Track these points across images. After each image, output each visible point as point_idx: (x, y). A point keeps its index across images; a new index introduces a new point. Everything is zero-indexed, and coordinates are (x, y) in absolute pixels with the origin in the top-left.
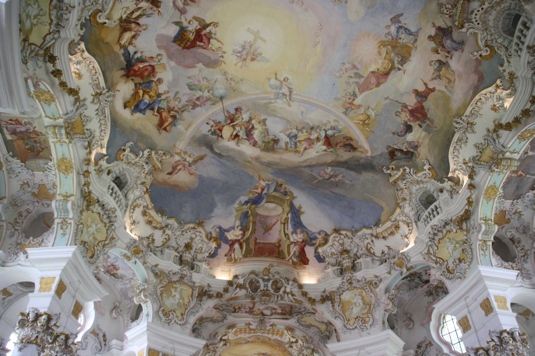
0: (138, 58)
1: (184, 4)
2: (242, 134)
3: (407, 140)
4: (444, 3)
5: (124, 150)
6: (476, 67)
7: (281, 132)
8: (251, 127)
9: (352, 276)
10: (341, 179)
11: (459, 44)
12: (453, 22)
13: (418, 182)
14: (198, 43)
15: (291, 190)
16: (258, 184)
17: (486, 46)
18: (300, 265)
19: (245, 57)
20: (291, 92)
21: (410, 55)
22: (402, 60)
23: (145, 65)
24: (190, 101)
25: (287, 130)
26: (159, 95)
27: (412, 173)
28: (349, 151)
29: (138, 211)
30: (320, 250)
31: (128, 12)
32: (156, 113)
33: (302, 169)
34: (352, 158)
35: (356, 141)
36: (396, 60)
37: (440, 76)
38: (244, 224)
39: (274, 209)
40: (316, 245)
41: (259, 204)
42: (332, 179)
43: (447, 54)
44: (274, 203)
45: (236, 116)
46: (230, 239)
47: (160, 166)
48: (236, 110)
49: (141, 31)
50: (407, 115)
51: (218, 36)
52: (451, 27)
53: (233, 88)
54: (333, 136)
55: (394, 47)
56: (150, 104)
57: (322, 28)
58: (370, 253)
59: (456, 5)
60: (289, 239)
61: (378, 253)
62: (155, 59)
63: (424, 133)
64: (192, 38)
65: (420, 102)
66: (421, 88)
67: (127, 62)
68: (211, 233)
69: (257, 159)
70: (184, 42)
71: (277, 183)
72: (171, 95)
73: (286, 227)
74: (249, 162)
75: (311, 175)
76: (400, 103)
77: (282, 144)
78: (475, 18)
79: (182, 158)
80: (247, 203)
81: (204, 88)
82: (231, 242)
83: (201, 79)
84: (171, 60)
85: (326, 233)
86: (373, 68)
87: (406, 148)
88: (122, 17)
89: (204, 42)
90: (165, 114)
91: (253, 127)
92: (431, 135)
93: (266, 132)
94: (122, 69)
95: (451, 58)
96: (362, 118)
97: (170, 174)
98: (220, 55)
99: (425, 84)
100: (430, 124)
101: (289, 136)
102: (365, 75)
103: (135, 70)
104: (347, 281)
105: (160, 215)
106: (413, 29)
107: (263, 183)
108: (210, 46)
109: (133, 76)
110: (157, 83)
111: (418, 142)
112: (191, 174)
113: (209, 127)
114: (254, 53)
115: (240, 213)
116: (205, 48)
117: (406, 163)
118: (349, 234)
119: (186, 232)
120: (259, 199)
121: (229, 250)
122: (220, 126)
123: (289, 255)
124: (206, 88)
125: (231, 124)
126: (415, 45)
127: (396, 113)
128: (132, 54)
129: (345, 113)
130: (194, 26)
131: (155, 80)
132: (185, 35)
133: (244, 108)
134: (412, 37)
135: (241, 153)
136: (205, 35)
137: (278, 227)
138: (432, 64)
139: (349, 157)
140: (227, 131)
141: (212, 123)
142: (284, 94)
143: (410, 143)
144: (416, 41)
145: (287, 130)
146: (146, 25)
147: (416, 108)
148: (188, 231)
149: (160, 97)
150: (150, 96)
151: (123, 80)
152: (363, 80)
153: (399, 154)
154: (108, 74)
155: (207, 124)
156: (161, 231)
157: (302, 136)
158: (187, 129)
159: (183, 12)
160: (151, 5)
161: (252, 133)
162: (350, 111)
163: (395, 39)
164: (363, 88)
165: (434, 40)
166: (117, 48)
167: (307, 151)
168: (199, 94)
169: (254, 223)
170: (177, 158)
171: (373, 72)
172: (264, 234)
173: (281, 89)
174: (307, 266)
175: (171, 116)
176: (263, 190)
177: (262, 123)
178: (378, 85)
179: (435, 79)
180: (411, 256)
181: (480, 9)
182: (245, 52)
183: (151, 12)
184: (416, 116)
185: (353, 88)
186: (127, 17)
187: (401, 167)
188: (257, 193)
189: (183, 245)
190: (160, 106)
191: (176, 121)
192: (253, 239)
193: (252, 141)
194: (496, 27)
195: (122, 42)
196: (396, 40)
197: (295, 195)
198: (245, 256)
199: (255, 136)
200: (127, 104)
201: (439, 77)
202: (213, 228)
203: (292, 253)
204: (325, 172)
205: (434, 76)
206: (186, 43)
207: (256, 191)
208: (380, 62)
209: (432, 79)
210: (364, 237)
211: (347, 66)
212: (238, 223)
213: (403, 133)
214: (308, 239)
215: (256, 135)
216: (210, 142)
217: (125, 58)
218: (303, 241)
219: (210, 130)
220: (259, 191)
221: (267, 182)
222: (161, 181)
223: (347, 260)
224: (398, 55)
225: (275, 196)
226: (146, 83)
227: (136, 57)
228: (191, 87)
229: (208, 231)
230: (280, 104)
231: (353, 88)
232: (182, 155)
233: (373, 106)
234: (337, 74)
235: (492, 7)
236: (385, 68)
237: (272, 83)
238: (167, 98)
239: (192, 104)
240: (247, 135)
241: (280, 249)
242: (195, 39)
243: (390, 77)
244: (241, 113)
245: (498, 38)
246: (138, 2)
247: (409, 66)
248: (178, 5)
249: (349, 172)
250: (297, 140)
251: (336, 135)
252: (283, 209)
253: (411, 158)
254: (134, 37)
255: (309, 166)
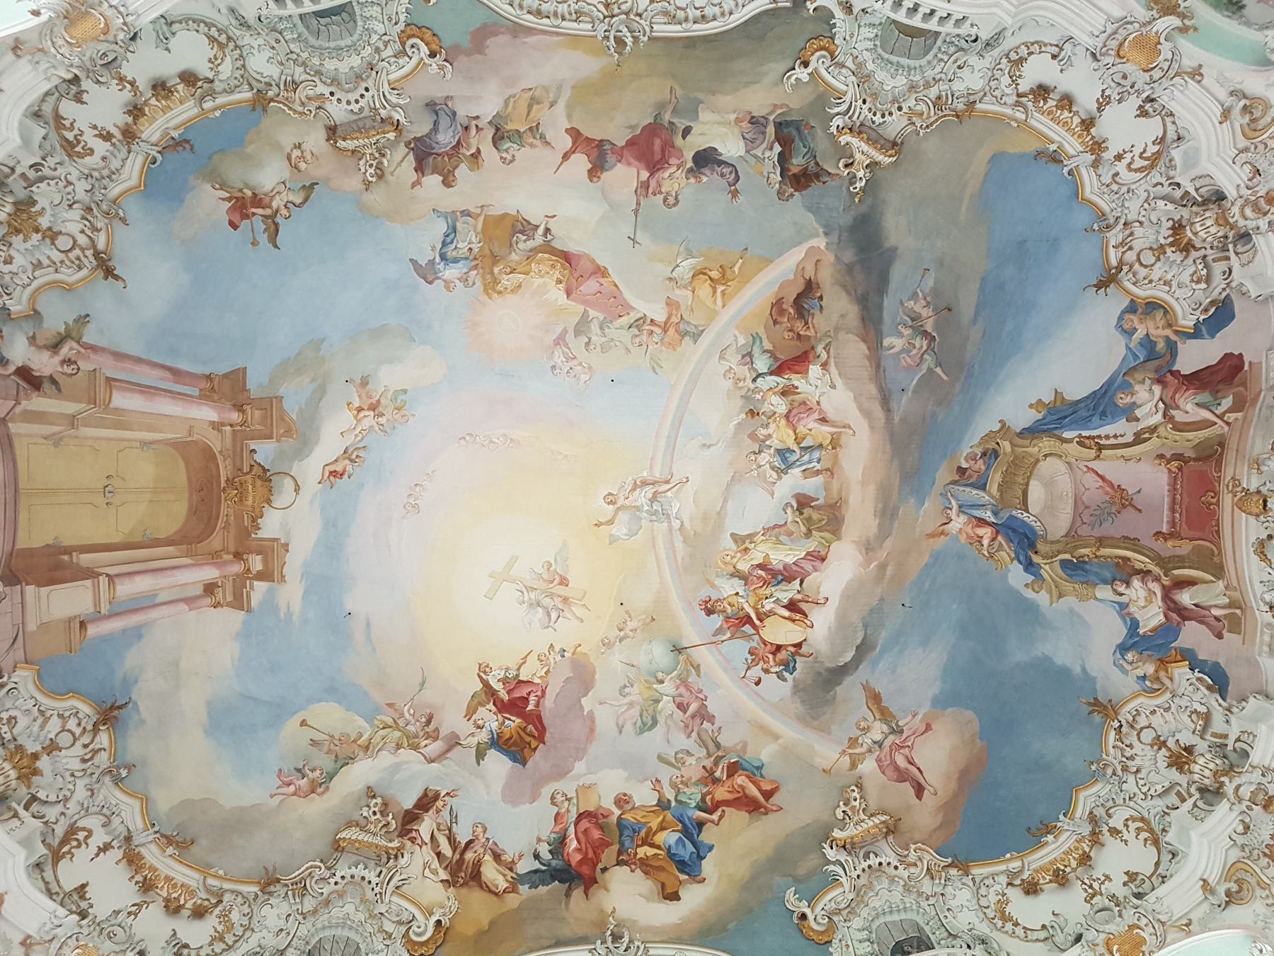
0: (550, 851)
1: (436, 739)
2: (787, 593)
3: (742, 152)
4: (361, 177)
5: (803, 917)
6: (469, 53)
7: (772, 495)
8: (760, 572)
9: (1239, 203)
10: (924, 303)
11: (436, 113)
12: (393, 145)
13: (864, 78)
14: (530, 707)
15: (976, 440)
16: (963, 538)
17: (403, 53)
18: (1244, 384)
19: (558, 601)
20: (645, 483)
21: (505, 215)
22: (522, 232)
23: (573, 836)
24: (687, 726)
25: (762, 477)
26: (663, 805)
27: (844, 107)
28: (821, 298)
29: (1020, 905)
30: (1187, 321)
31: (435, 864)
32: (715, 817)
33: (897, 419)
34: (844, 287)
35: (782, 287)
36: (524, 245)
37: (531, 129)
38: (1108, 575)
39: (1049, 484)
40: (1173, 337)
41: (1032, 529)
42: (929, 327)
43: (473, 131)
44: (1027, 484)
45: (729, 611)
46: (1162, 617)
47: (883, 818)
48: (709, 612)
49: (488, 839)
50: (666, 175)
51: (514, 666)
52: (407, 144)
53: (646, 624)
54: (773, 355)
55: (495, 259)
56: (686, 832)
57: (470, 435)
58: (1157, 155)
59: (353, 152)
60: (1153, 430)
61: (1153, 127)
62: (563, 810)
63: (704, 116)
64: (518, 721)
65: (620, 154)
66: (581, 163)
67: (553, 879)
68: (1144, 677)
69: (868, 548)
70: (528, 739)
71: (954, 483)
72: (666, 774)
73: (1112, 441)
74: (883, 567)
75: (915, 391)
76: (638, 204)
77: (812, 486)
78: (357, 101)
79: (870, 751)
80: (1029, 566)
81: (648, 694)
82: (1174, 616)
83: (627, 700)
84: (570, 771)
85: (1123, 313)
86: (557, 294)
87: (771, 149)
88: (442, 881)
89: (529, 694)
90: (721, 793)
91: (761, 566)
92: (700, 96)
93: (775, 531)
94: (568, 895)
95: (477, 117)
96: (704, 289)
97: (919, 790)
98: (558, 658)
99: (566, 157)
100: (671, 108)
101: (781, 472)
102: (581, 308)
103: (581, 862)
104: (1265, 214)
105: (1050, 838)
106: (442, 227)
107: (959, 523)
108: (537, 681)
109: (595, 866)
110: (628, 807)
111: (738, 121)
112: (928, 728)
113: (770, 680)
114: (545, 581)
115: (1067, 586)
116: (544, 692)
117: (819, 132)
118: (1115, 236)
119: (1132, 758)
120: (1014, 531)
121: (1201, 622)
122: (762, 650)
123: (1208, 424)
124: (649, 688)
125: (757, 622)
126: (479, 211)
127: (669, 206)
128: (537, 865)
129: (696, 337)
130: (490, 719)
131: (617, 812)
132: (510, 738)
133: (704, 593)
134: (459, 226)
135: (850, 595)
136: (509, 692)
137: (1113, 467)
138: (509, 157)
139: (843, 295)
140: (781, 631)
141: (756, 672)
142: (654, 499)
143: (750, 143)
144: (466, 213)
145: (762, 477)
146: (475, 825)
147: (639, 159)
148: (1128, 752)
149: (669, 801)
150: (662, 828)
151: (598, 895)
152: (592, 313)
153: (797, 162)
154: (567, 932)
155: (757, 683)
156: (1111, 843)
157: (781, 435)
158: (776, 737)
159: (454, 742)
160: (431, 812)
161: (781, 567)
162: (689, 323)
163: (474, 263)
164: (615, 304)
165: (452, 172)
166: (513, 901)
167: (831, 415)
168: (667, 705)
169: (1101, 542)
170: (868, 766)
171: (569, 294)
172: (1140, 511)
173: (638, 508)
174: (1246, 360)
175: (730, 775)
176: (982, 522)
177: (747, 544)
178: (601, 272)
179: (542, 137)
180: (1098, 22)
181: (334, 99)
182: (547, 602)
183: (445, 814)
184: (663, 151)
185: (619, 331)
186: (446, 868)
187: (836, 143)
188: (993, 539)
189: (1174, 774)
190: (693, 805)
191: (746, 765)
192: (1159, 545)
193: (808, 566)
194: (353, 48)
195: (503, 885)
196: (475, 259)
197: (997, 427)
198: (1218, 571)
199: (790, 560)
200: (669, 890)
201: (534, 130)
202: (1125, 672)
203: (1206, 414)
204: (903, 351)
205: (537, 142)
206: (531, 735)
207: (986, 542)
208: (538, 281)
209: (548, 143)
210: (1115, 187)
211: (559, 358)
212: (1104, 592)
213: (726, 170)
214: (1153, 365)
215: (782, 556)
216: (820, 674)
217: (544, 883)
218: (1159, 381)
219: (780, 676)
220: (986, 532)
221: (953, 514)
222: (939, 819)
223: (1198, 227)
224: (511, 245)
225: (1000, 485)
226: (621, 835)
227: (546, 856)
228: (648, 723)
229: (1137, 687)
230: (683, 505)
231: (619, 331)
232: (858, 750)
233: (664, 270)
234: (584, 377)
235: (319, 73)
236: (553, 266)
237: (625, 531)
238: (673, 785)
239: (698, 721)
240: (789, 579)
241: (1190, 454)
242: (522, 714)
243: (571, 247)
244: (717, 601)
245: (376, 32)
246: (419, 841)
247: (534, 211)
248: (437, 753)
249: (892, 286)
250: (795, 448)
251: (768, 346)
252: (1046, 456)
253: (797, 125)
254: (497, 857)
255: (885, 401)
